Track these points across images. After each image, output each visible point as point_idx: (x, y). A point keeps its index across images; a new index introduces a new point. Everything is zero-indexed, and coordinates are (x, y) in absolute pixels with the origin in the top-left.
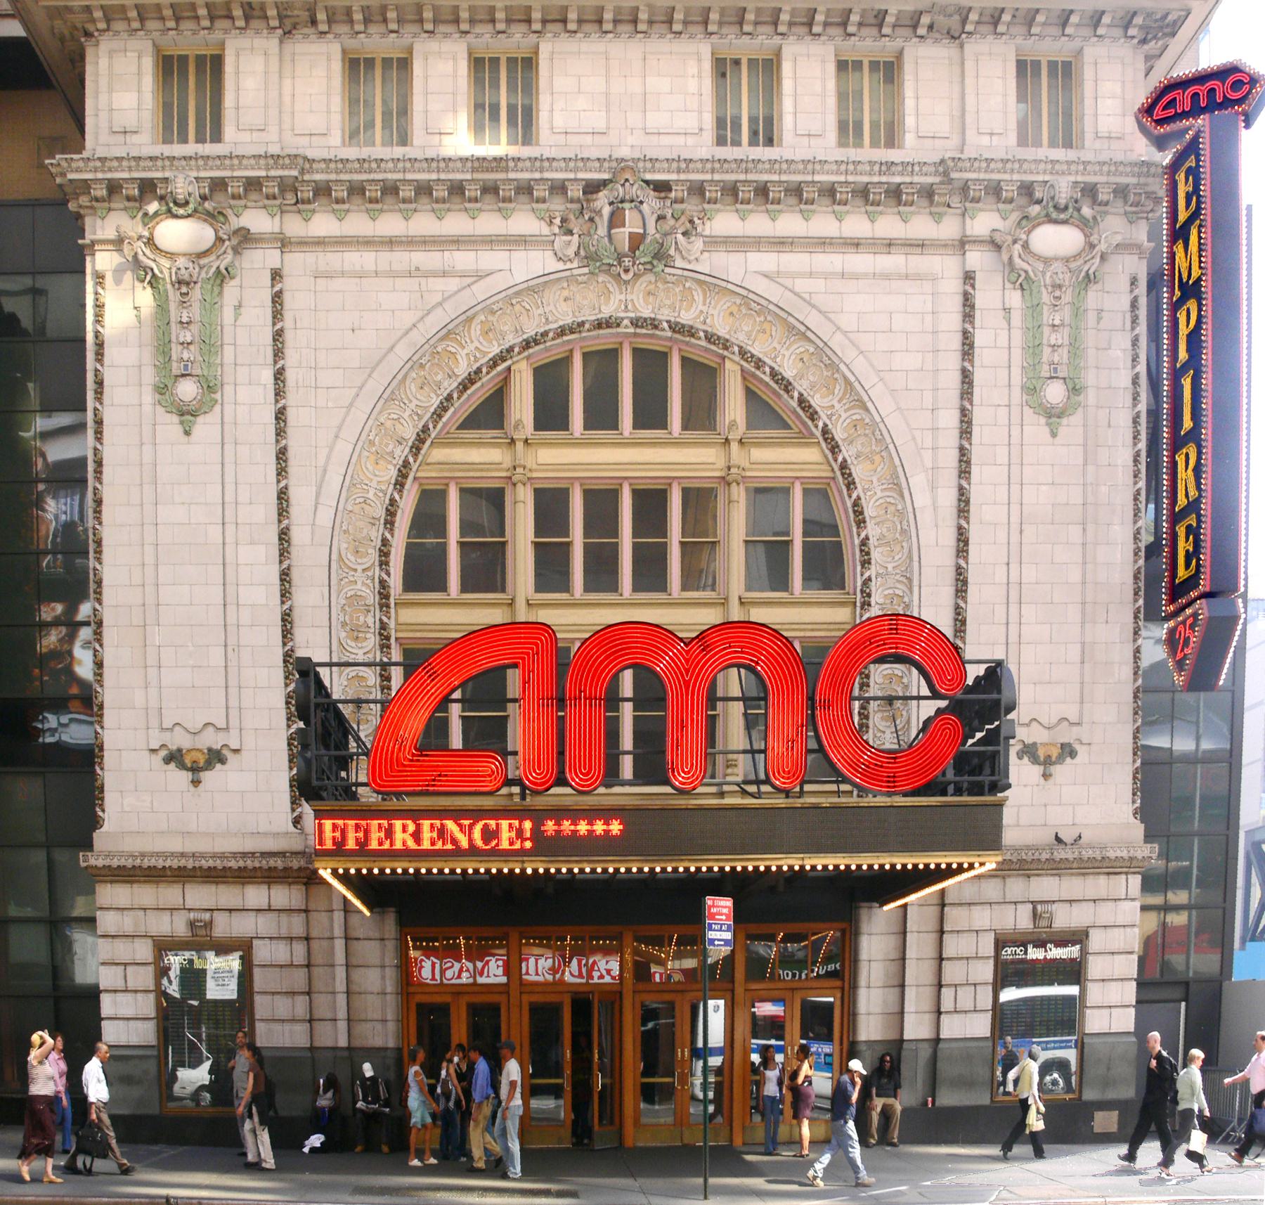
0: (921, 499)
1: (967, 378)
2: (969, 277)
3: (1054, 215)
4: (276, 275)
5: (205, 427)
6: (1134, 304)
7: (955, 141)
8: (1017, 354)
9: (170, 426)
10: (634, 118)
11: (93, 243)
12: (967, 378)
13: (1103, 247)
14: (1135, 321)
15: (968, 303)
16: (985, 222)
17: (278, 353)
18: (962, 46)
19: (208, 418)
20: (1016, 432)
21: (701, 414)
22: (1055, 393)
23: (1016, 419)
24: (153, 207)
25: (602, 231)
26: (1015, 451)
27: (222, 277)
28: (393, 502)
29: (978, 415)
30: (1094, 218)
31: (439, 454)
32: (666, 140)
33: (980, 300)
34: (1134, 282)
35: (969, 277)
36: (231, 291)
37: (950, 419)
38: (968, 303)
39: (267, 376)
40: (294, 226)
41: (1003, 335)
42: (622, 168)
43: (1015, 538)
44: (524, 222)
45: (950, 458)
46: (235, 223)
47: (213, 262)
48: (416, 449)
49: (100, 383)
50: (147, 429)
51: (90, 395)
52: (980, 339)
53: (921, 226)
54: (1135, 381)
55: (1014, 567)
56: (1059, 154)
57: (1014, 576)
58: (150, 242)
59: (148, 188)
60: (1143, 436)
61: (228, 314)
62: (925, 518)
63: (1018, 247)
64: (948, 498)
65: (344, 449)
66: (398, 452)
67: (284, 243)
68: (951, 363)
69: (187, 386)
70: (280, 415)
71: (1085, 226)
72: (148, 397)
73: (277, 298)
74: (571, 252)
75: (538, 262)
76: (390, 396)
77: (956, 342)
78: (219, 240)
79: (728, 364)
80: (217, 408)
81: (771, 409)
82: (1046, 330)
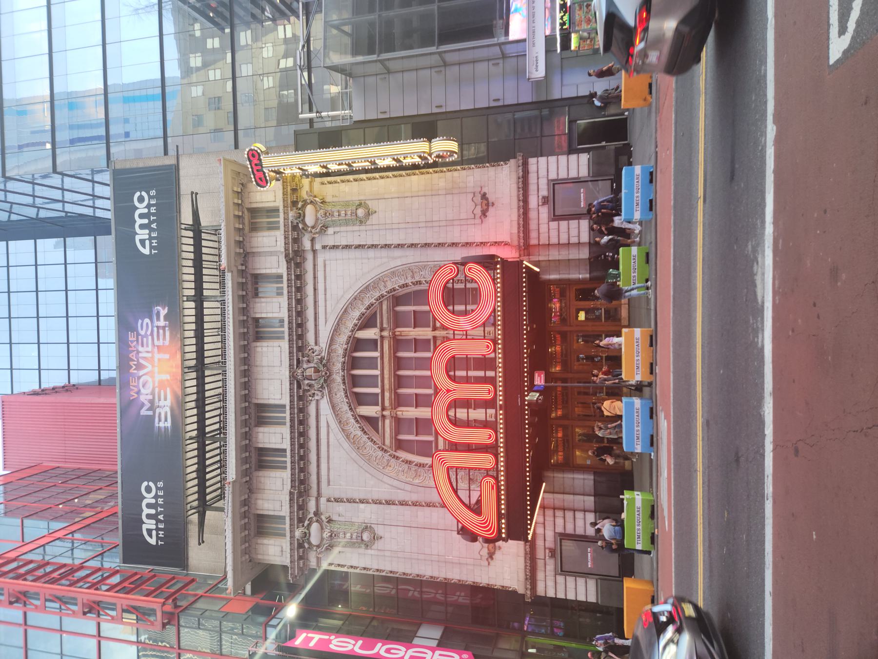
1: (359, 247)
4: (329, 500)
6: (330, 183)
8: (349, 228)
9: (378, 544)
10: (277, 370)
15: (334, 247)
18: (248, 253)
20: (374, 227)
21: (372, 344)
22: (361, 212)
24: (306, 545)
25: (313, 382)
27: (330, 521)
28: (403, 461)
29: (370, 243)
31: (388, 442)
33: (331, 243)
34: (323, 184)
35: (324, 247)
36: (335, 518)
38: (334, 247)
39: (362, 506)
40: (314, 491)
41: (342, 234)
42: (293, 377)
43: (410, 225)
45: (384, 252)
46: (312, 515)
47: (325, 523)
51: (368, 572)
52: (344, 243)
53: (309, 265)
54: (356, 180)
55: (421, 225)
56: (282, 215)
57: (423, 225)
58: (318, 546)
59: (300, 546)
61: (341, 519)
62: (405, 261)
64: (398, 253)
65: (386, 479)
67: (319, 495)
68: (353, 253)
69: (366, 538)
71: (305, 203)
72: (369, 551)
73: (337, 500)
74: (320, 394)
75: (325, 405)
76: (368, 460)
77: (345, 251)
78: (317, 521)
79: (356, 336)
81: (368, 322)
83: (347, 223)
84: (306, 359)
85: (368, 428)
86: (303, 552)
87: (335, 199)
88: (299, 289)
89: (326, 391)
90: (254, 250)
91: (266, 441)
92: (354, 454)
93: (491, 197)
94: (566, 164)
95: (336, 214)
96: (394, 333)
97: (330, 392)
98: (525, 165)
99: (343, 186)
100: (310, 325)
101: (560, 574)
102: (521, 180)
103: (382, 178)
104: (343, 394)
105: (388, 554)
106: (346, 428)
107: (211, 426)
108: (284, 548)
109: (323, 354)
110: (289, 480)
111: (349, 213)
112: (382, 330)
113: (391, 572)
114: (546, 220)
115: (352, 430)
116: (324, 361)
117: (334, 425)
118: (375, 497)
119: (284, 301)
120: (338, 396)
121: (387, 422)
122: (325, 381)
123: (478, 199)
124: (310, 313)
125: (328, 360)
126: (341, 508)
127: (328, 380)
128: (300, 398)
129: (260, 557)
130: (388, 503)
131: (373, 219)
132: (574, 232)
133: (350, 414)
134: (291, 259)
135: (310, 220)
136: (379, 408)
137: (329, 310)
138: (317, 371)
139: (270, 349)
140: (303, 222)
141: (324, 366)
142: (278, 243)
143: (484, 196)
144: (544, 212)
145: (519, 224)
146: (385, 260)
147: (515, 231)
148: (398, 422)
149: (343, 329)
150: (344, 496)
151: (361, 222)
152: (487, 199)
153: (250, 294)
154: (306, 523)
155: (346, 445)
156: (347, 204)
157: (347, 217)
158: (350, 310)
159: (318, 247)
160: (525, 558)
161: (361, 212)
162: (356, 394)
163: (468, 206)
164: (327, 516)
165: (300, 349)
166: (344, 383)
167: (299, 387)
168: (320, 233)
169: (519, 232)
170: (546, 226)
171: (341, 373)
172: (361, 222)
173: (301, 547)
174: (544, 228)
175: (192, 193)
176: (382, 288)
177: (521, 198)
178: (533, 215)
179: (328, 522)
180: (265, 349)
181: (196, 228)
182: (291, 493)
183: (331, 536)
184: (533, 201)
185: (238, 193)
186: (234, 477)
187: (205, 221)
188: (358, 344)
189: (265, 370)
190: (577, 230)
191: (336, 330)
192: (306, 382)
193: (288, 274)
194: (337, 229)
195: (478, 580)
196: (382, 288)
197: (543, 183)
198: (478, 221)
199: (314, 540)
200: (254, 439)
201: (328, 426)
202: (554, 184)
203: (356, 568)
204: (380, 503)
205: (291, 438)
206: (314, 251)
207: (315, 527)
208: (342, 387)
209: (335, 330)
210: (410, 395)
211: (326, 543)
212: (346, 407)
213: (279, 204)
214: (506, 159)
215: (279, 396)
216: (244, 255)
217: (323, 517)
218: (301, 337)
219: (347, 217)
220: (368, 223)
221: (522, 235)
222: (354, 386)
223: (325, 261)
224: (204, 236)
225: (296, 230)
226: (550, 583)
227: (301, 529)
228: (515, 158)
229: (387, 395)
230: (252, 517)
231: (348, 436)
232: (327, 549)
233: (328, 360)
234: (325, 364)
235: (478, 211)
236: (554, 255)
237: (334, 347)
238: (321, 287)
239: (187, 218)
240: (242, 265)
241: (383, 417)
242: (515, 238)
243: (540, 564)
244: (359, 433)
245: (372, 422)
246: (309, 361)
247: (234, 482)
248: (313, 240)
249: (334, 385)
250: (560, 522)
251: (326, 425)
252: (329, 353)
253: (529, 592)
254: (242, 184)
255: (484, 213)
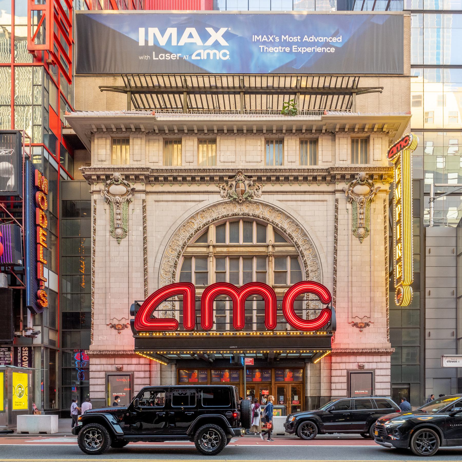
0: (323, 260)
1: (336, 228)
2: (337, 201)
3: (361, 182)
4: (144, 201)
5: (124, 242)
6: (385, 207)
7: (333, 162)
8: (350, 221)
9: (114, 242)
10: (243, 158)
11: (94, 191)
12: (336, 228)
13: (374, 191)
14: (385, 211)
15: (337, 208)
16: (341, 186)
17: (144, 222)
18: (335, 136)
19: (124, 239)
20: (350, 241)
21: (262, 238)
22: (362, 231)
23: (350, 239)
24: (108, 182)
25: (234, 189)
26: (350, 247)
27: (129, 201)
28: (176, 261)
29: (339, 237)
30: (372, 183)
32: (251, 164)
33: (340, 207)
34: (385, 201)
35: (337, 201)
36: (131, 205)
37: (331, 239)
38: (337, 208)
39: (141, 228)
40: (149, 188)
41: (346, 216)
42: (239, 172)
43: (350, 270)
44: (213, 187)
45: (331, 249)
46: (132, 187)
47: (126, 197)
48: (183, 248)
49: (95, 230)
50: (107, 242)
51: (92, 233)
52: (340, 217)
53: (324, 187)
54: (385, 228)
55: (350, 278)
57: (350, 280)
58: (108, 192)
59: (108, 177)
60: (388, 242)
61: (130, 211)
62: (324, 265)
63: (350, 191)
64: (331, 260)
65: (162, 248)
66: (178, 248)
67: (147, 193)
68: (331, 224)
70: (145, 238)
71: (371, 185)
72: (108, 234)
73: (144, 207)
74: (225, 194)
75: (216, 198)
76: (176, 234)
77: (333, 218)
78: (128, 191)
79: (269, 225)
80: (127, 237)
82: (358, 214)
83: (355, 219)
84: (252, 183)
85: (200, 233)
86: (103, 179)
87: (372, 210)
88: (305, 179)
89: (227, 200)
90: (337, 140)
91: (188, 148)
92: (179, 222)
93: (366, 330)
94: (384, 381)
95: (362, 211)
96: (270, 256)
97: (226, 203)
98: (387, 354)
99: (381, 217)
100: (277, 187)
101: (106, 374)
102: (377, 351)
103: (386, 249)
104: (225, 214)
105: (108, 248)
106: (199, 216)
107: (196, 100)
108: (104, 163)
109: (255, 198)
110: (157, 168)
111: (362, 221)
112: (273, 246)
113: (94, 251)
114: (348, 368)
115: (198, 221)
116: (250, 199)
117: (201, 206)
118: (149, 239)
119: (296, 166)
120: (223, 210)
121: (204, 250)
122: (235, 199)
123: (367, 321)
124: (286, 187)
125: (250, 202)
126: (139, 211)
127: (235, 201)
128: (221, 178)
129: (96, 141)
130: (145, 249)
131: (356, 241)
132: (339, 386)
133: (210, 219)
134: (329, 172)
135: (359, 189)
136: (215, 243)
137: (289, 203)
138: (243, 192)
139: (259, 153)
140: (358, 184)
141: (246, 198)
142: (342, 162)
143: (367, 325)
144: (354, 367)
145: (347, 349)
146: (325, 251)
147: (342, 346)
148: (205, 258)
149: (275, 214)
150: (148, 213)
151: (354, 231)
152: (365, 327)
153: (302, 136)
154: (125, 181)
155: (187, 216)
156: (368, 220)
157: (358, 220)
158: (288, 220)
159: (338, 195)
160: (114, 351)
161: (362, 231)
162: (224, 224)
163: (361, 314)
164: (132, 200)
165: (259, 179)
166: (233, 215)
167: (230, 177)
168: (348, 197)
169: (341, 349)
170: (344, 368)
171: (241, 213)
172: (354, 231)
173: (107, 178)
174: (343, 366)
175: (382, 88)
176: (304, 247)
177: (364, 351)
178: (352, 359)
179: (127, 200)
180: (259, 148)
181: (349, 92)
182: (148, 169)
183: (117, 203)
184: (361, 359)
185: (382, 129)
186: (159, 119)
187: (358, 99)
188: (262, 225)
189: (243, 148)
190: (340, 388)
191: (273, 209)
192: (234, 183)
193: (318, 169)
194: (350, 212)
195: (95, 317)
196: (304, 247)
197: (374, 366)
198: (350, 320)
199: (113, 189)
200: (188, 137)
201: (200, 201)
202: (372, 373)
203: (95, 222)
204: (144, 243)
205: (190, 170)
206: (334, 192)
207: (123, 189)
208: (230, 213)
209: (273, 208)
210: (225, 268)
211: (112, 198)
212: (215, 216)
213: (372, 164)
214: (391, 341)
215: (222, 160)
216: (333, 132)
217: (130, 196)
218: (269, 179)
219: (358, 220)
220: (354, 237)
221: (339, 351)
222: (231, 223)
223: (326, 201)
224: (347, 97)
225: (350, 177)
226: (99, 368)
227: (121, 178)
228: (392, 347)
229: (225, 249)
230: (126, 135)
231: (193, 217)
232: (107, 199)
233: (250, 202)
234: (248, 200)
235: (357, 321)
236: (324, 373)
237: (261, 206)
238: (307, 197)
239: (364, 83)
240: (326, 130)
241: (208, 246)
242: (338, 347)
243: (112, 361)
244: (196, 227)
245: (204, 236)
246: (250, 186)
247: (154, 119)
248: (343, 191)
249: (231, 206)
250: (142, 375)
251: (201, 199)
252: (256, 203)
253: (91, 353)
254: (388, 133)
255: (355, 325)
